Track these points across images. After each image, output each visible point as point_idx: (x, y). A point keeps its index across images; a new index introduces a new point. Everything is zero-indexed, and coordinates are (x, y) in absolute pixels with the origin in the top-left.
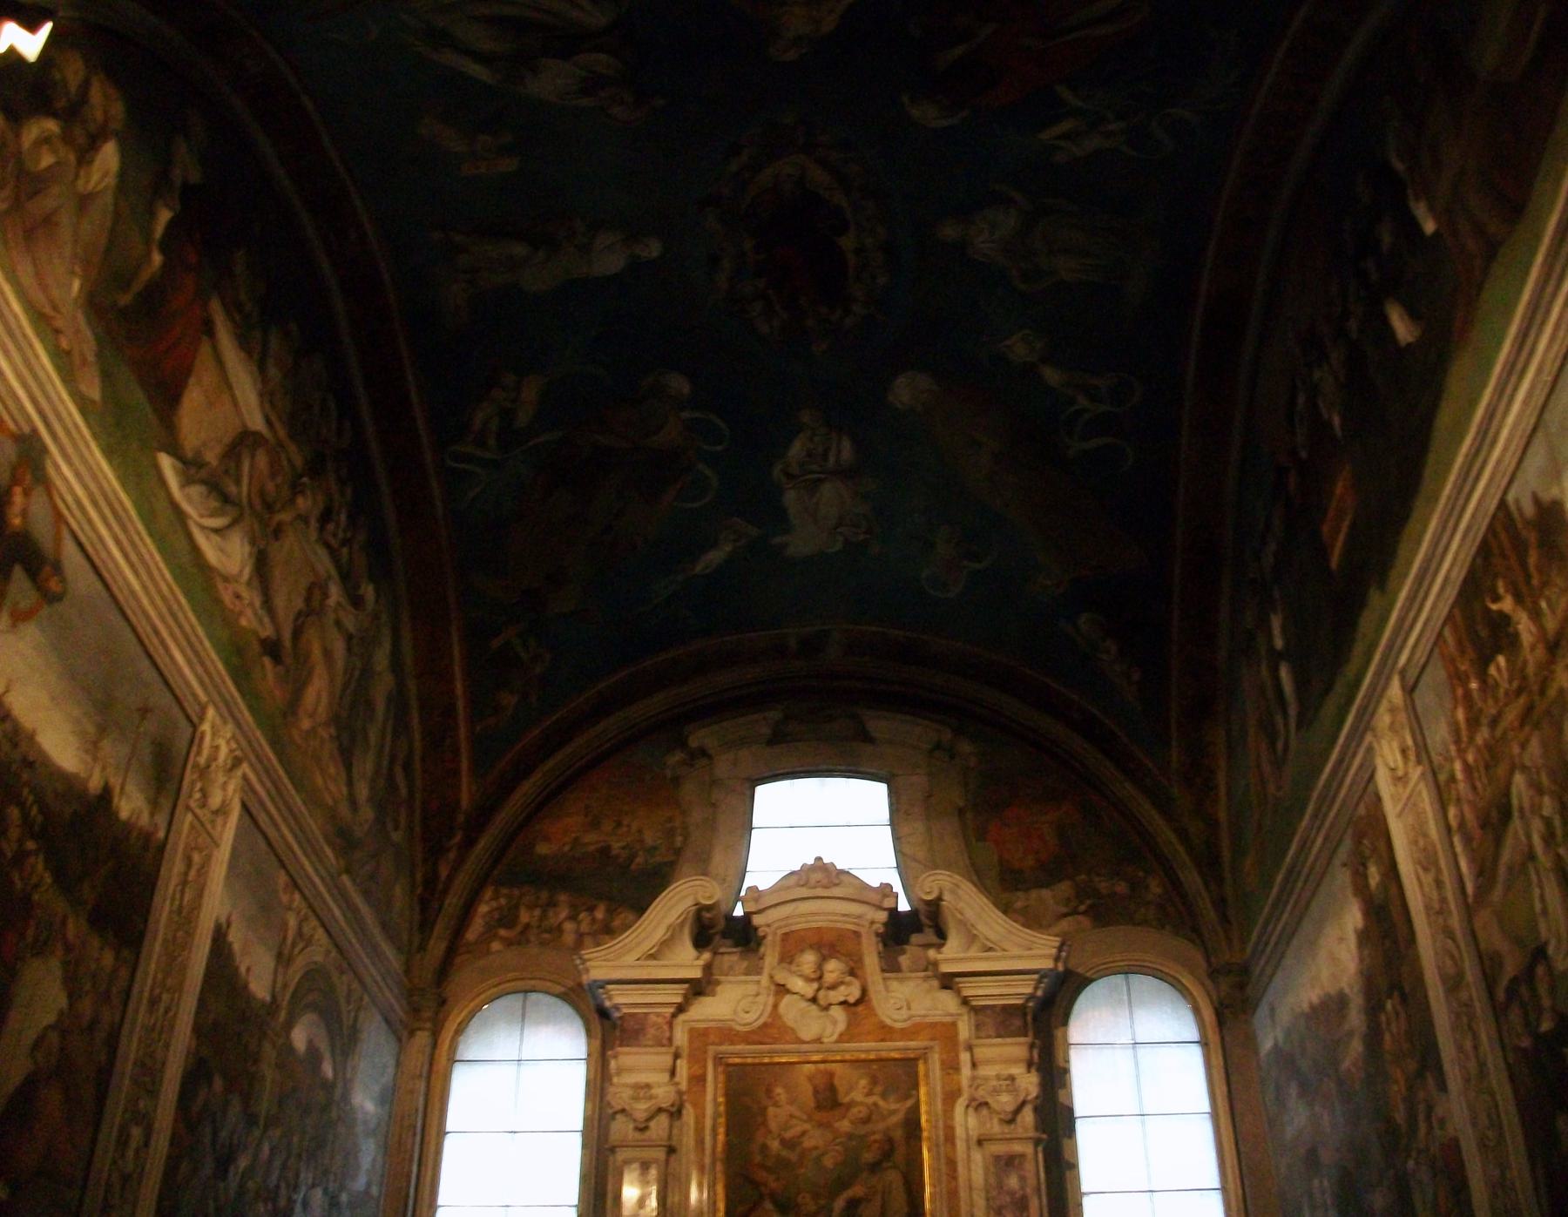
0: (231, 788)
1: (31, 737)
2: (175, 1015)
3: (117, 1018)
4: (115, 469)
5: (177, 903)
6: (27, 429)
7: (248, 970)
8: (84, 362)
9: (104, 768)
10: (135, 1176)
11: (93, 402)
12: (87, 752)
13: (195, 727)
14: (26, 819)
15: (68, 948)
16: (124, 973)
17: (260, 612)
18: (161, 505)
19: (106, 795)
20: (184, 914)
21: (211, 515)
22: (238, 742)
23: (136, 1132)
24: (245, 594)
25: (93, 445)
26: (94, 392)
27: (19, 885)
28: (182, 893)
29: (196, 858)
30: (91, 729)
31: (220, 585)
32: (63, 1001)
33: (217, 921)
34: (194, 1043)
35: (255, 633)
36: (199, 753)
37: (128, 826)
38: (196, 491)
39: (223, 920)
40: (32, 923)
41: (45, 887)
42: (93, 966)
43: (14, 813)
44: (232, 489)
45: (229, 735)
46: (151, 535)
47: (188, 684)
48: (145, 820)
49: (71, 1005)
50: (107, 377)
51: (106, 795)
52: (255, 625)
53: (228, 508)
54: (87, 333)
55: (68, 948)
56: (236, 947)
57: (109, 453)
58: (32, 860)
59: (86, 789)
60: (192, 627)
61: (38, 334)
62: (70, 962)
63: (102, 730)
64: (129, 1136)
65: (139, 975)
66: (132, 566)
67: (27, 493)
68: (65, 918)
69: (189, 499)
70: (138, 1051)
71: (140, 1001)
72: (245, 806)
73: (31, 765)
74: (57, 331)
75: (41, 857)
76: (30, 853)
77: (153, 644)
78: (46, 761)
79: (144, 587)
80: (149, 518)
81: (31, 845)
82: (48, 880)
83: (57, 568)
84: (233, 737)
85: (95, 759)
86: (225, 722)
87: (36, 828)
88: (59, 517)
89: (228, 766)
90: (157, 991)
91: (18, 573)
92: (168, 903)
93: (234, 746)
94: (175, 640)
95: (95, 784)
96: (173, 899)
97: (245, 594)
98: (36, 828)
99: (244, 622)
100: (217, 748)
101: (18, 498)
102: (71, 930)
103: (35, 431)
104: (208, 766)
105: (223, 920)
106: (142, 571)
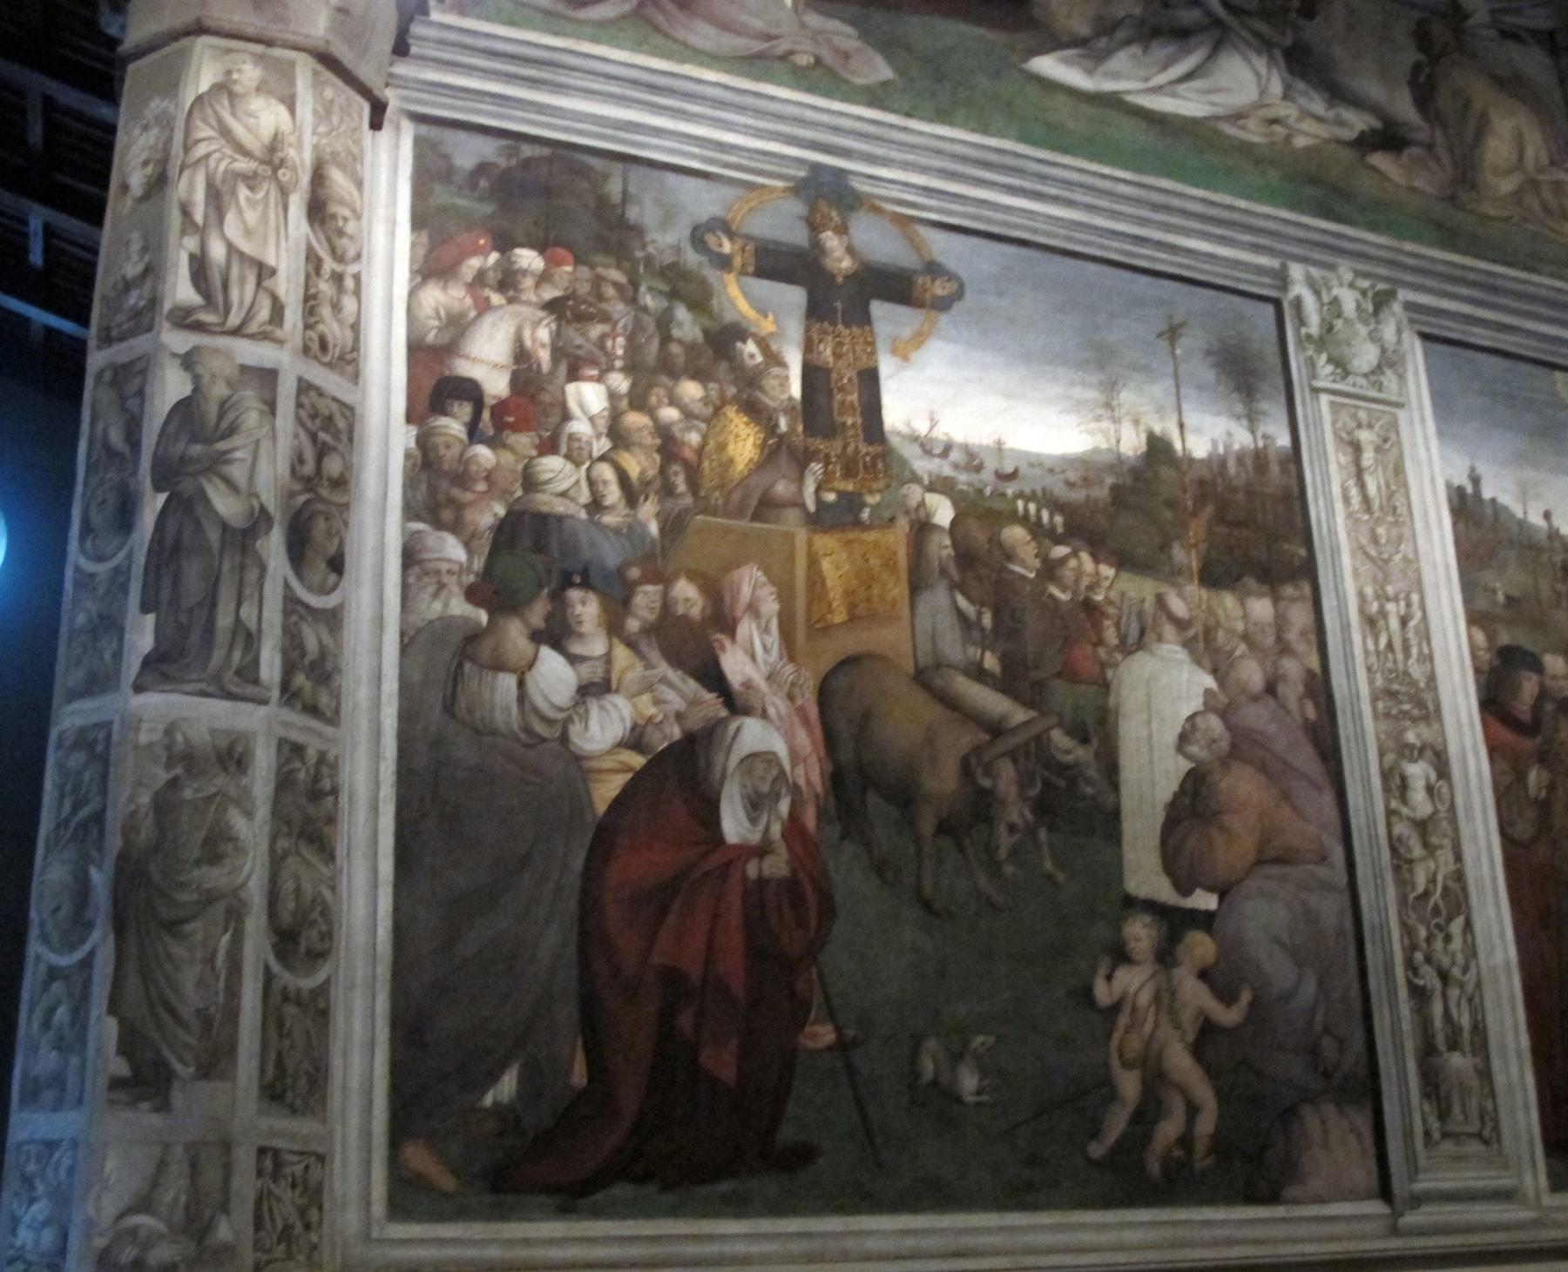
0: (1389, 333)
1: (999, 448)
2: (1425, 617)
3: (1314, 662)
4: (964, 125)
5: (1356, 499)
6: (802, 174)
7: (1547, 515)
8: (846, 56)
9: (1136, 422)
10: (1442, 814)
11: (886, 84)
12: (1098, 419)
13: (1277, 304)
14: (1037, 530)
15: (1181, 625)
16: (1299, 616)
17: (1331, 114)
18: (1061, 108)
19: (1157, 448)
20: (1376, 506)
21: (1165, 67)
22: (1366, 275)
23: (1418, 772)
24: (1288, 111)
25: (913, 124)
26: (882, 70)
27: (1063, 597)
28: (1362, 486)
29: (1365, 436)
30: (1092, 394)
31: (1229, 129)
32: (1209, 681)
33: (1449, 485)
34: (1480, 637)
35: (1339, 141)
36: (1301, 321)
37: (1218, 464)
38: (1122, 60)
39: (1462, 479)
40: (1107, 623)
41: (1107, 583)
42: (1240, 626)
43: (1015, 534)
44: (1191, 16)
45: (1348, 276)
46: (1065, 151)
47: (1236, 264)
48: (1242, 438)
49: (1221, 682)
50: (887, 46)
51: (1157, 448)
52: (1323, 131)
53: (1193, 40)
54: (834, 25)
55: (1181, 625)
56: (1507, 499)
57: (942, 115)
58: (1072, 563)
59: (1119, 457)
60: (1204, 201)
61: (757, 79)
62: (1195, 638)
63: (1111, 387)
64: (1404, 779)
65: (1328, 603)
66: (1055, 200)
67: (842, 230)
68: (1161, 601)
69: (1115, 75)
70: (1371, 682)
71: (1346, 628)
72: (1425, 337)
73: (1013, 476)
74: (784, 58)
75: (1085, 556)
76: (1062, 561)
77: (1144, 257)
78: (1036, 462)
79: (1090, 208)
80: (1057, 138)
81: (1060, 551)
82: (1108, 571)
83: (934, 269)
84: (1358, 274)
85: (1116, 421)
86: (1331, 267)
87: (1060, 530)
88: (904, 222)
89: (1370, 308)
90: (1375, 607)
91: (878, 309)
92: (1339, 506)
93: (1365, 284)
94: (1188, 232)
95: (1131, 443)
96: (1346, 499)
97: (1288, 111)
98: (1060, 530)
99: (1300, 142)
100: (1335, 301)
101: (831, 240)
102: (1178, 606)
103: (816, 168)
104: (1330, 328)
105: (1462, 479)
106: (1078, 197)
